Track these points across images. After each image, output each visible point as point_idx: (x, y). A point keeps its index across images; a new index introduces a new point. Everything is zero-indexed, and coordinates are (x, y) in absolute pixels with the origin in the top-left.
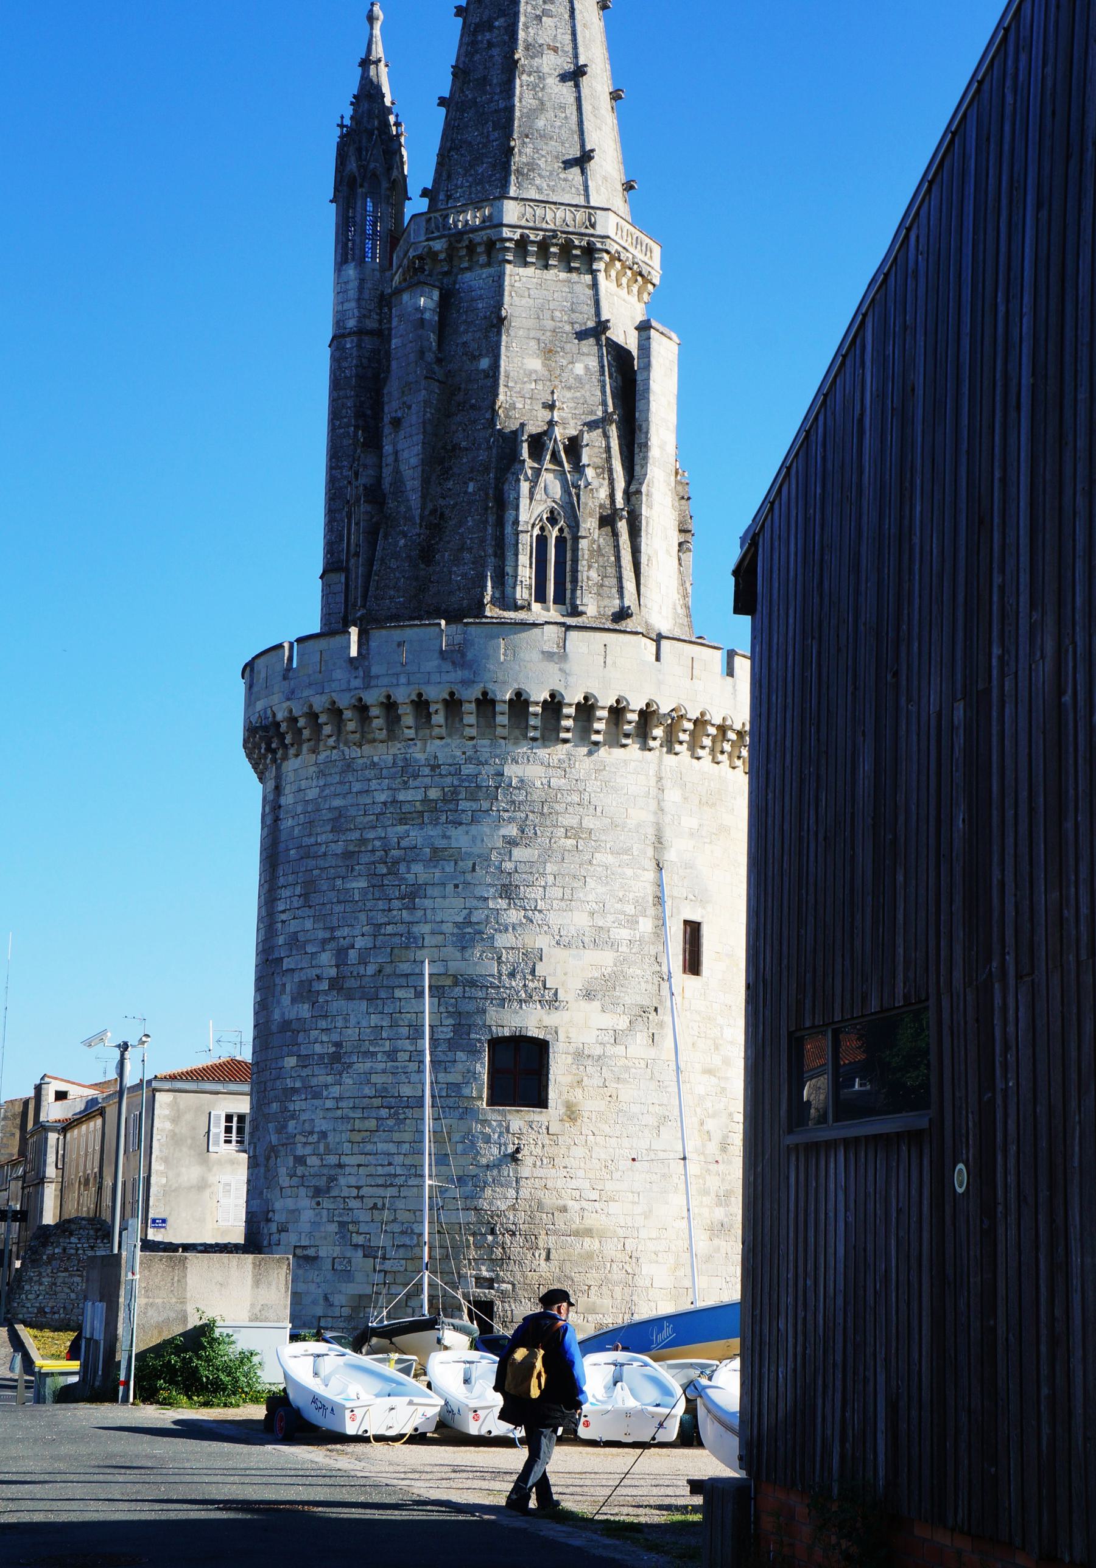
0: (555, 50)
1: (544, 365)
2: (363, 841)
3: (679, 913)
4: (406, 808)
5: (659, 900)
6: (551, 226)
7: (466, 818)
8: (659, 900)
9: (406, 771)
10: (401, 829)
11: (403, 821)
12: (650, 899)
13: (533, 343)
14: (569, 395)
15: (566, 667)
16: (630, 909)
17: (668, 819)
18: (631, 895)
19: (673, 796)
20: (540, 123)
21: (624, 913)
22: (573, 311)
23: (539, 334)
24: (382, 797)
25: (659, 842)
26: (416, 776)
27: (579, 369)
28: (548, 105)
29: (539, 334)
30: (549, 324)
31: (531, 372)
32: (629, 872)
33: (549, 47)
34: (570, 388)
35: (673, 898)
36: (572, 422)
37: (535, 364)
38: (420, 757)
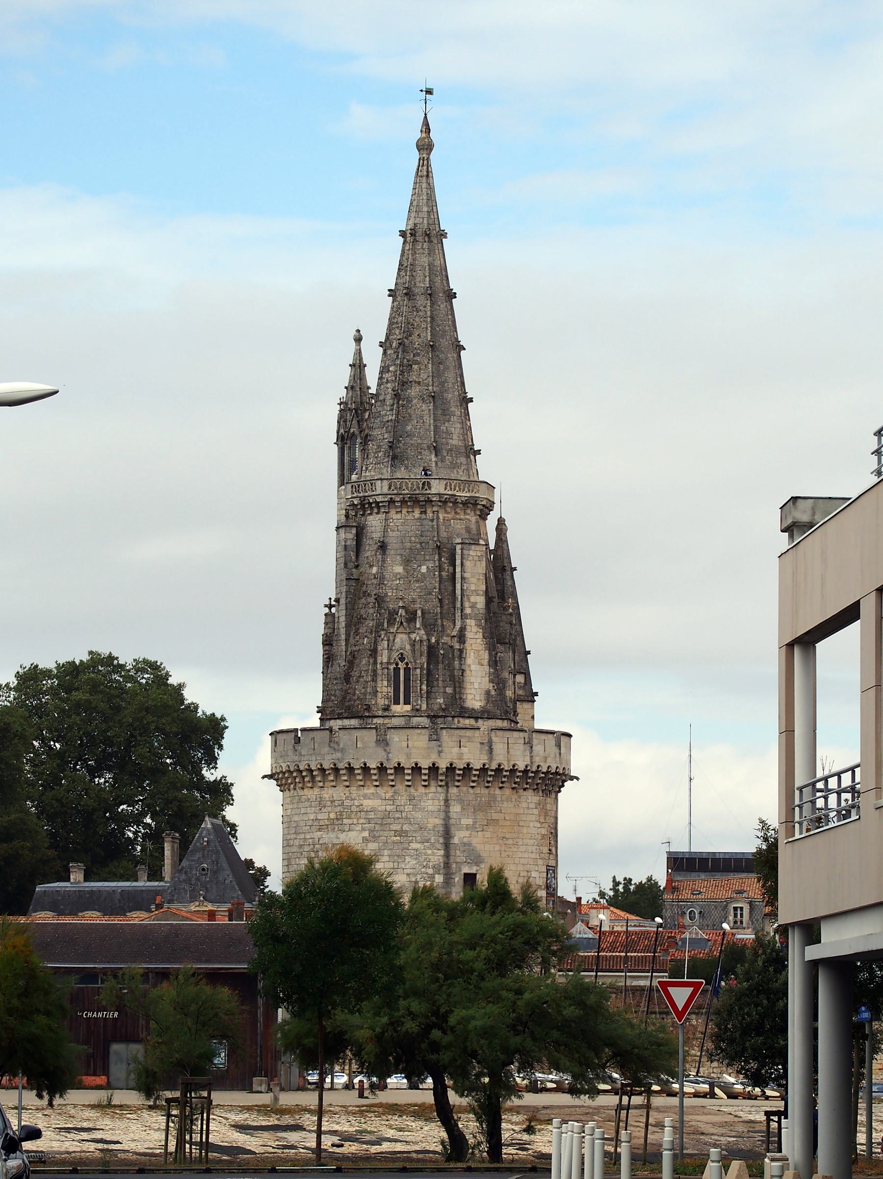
0: (419, 383)
1: (404, 569)
2: (305, 839)
3: (460, 870)
4: (322, 823)
5: (447, 865)
6: (406, 492)
7: (347, 828)
8: (447, 865)
9: (321, 804)
10: (319, 833)
11: (320, 830)
12: (442, 865)
13: (398, 557)
14: (417, 585)
15: (388, 749)
16: (430, 871)
17: (452, 821)
18: (431, 864)
19: (455, 808)
20: (409, 428)
21: (427, 873)
22: (422, 536)
23: (402, 552)
24: (312, 817)
25: (447, 835)
26: (325, 807)
27: (424, 569)
28: (413, 416)
29: (402, 552)
30: (408, 545)
31: (397, 574)
32: (429, 852)
33: (415, 382)
34: (417, 581)
35: (457, 863)
36: (419, 601)
37: (399, 569)
38: (326, 796)
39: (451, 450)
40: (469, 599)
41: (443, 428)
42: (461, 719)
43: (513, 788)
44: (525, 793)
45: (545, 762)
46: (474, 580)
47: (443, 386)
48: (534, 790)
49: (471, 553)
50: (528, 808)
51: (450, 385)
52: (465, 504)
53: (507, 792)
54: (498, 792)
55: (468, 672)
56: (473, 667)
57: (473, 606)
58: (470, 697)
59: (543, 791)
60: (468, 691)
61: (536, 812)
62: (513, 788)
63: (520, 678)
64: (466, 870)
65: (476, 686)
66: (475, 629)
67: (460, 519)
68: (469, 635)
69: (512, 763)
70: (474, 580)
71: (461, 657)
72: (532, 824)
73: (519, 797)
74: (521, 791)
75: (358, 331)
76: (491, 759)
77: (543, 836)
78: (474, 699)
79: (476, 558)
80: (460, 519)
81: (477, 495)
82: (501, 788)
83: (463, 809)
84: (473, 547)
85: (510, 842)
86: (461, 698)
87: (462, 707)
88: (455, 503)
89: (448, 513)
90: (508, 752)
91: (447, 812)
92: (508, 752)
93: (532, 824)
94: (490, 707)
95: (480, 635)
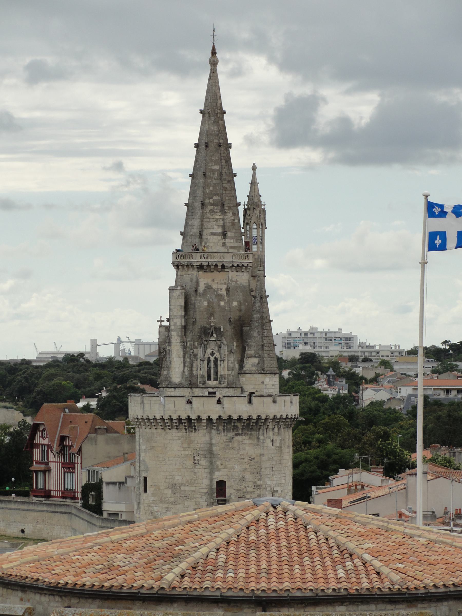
39: (192, 235)
40: (173, 321)
41: (190, 223)
42: (167, 389)
43: (162, 429)
44: (170, 431)
45: (175, 413)
46: (175, 310)
47: (195, 199)
48: (177, 429)
49: (174, 294)
50: (173, 440)
51: (198, 198)
52: (187, 266)
53: (159, 430)
54: (154, 431)
55: (172, 362)
56: (175, 359)
57: (175, 325)
58: (174, 376)
59: (186, 429)
60: (173, 373)
61: (178, 441)
62: (162, 429)
63: (256, 360)
64: (144, 475)
65: (177, 370)
66: (176, 337)
67: (189, 275)
68: (173, 341)
69: (153, 414)
70: (175, 310)
71: (169, 354)
72: (175, 449)
73: (167, 434)
74: (168, 430)
75: (254, 164)
76: (144, 412)
77: (187, 456)
78: (176, 378)
79: (176, 297)
80: (189, 275)
81: (192, 260)
82: (156, 429)
83: (143, 440)
84: (175, 291)
85: (161, 459)
86: (169, 377)
87: (170, 382)
88: (183, 266)
89: (182, 272)
90: (151, 409)
91: (140, 442)
92: (151, 409)
93: (175, 449)
94: (184, 382)
95: (179, 341)
